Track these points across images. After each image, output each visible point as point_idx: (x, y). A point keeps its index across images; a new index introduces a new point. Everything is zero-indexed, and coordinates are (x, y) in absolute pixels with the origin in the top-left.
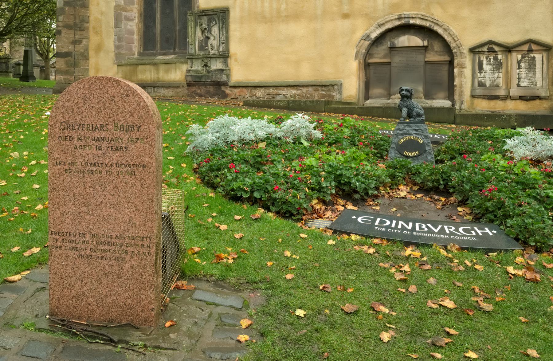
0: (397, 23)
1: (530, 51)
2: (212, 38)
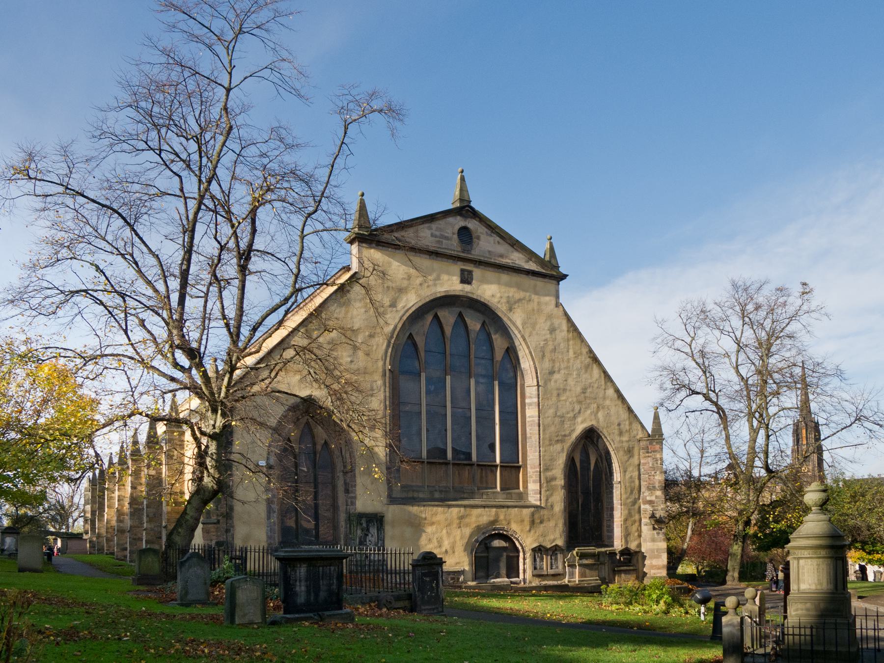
2: (370, 535)
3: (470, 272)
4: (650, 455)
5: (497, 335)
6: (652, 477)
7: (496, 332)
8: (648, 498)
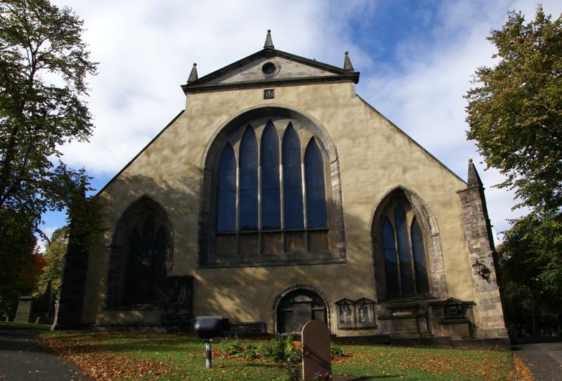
0: (295, 289)
1: (365, 303)
3: (272, 90)
4: (469, 204)
5: (302, 130)
6: (474, 225)
7: (301, 128)
8: (474, 247)
